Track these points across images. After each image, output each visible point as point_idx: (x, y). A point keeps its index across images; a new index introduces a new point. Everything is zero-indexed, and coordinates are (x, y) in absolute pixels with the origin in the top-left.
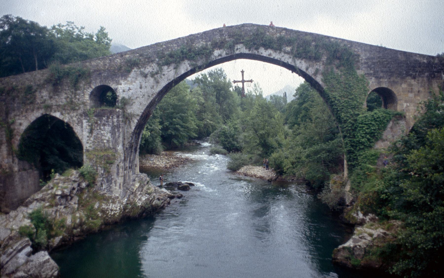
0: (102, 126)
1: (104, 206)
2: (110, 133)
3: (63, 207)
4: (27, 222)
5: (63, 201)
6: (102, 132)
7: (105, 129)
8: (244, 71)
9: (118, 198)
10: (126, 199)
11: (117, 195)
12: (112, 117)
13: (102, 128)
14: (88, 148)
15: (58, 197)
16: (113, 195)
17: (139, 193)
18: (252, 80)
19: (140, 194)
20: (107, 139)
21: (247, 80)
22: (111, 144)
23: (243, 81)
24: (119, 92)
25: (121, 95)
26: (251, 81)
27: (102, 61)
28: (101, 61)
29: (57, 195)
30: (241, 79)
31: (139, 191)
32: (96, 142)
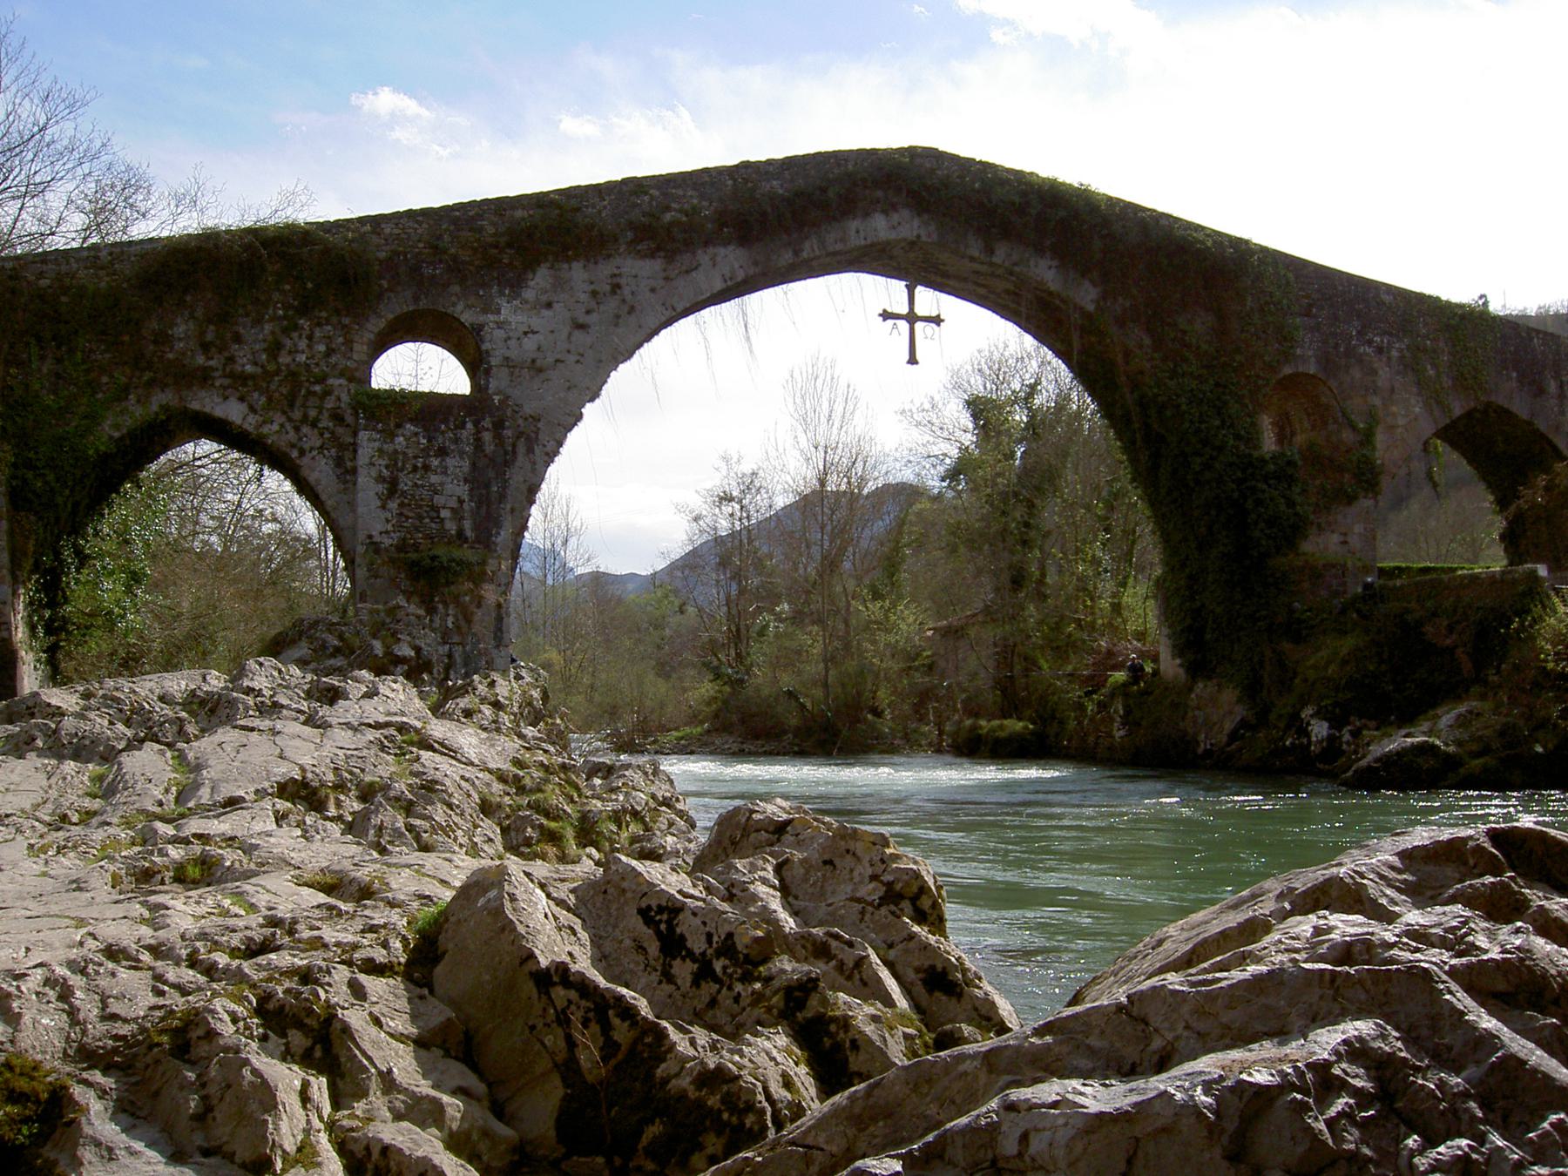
0: (436, 456)
2: (466, 481)
6: (434, 479)
7: (446, 468)
12: (476, 423)
13: (435, 462)
14: (377, 539)
18: (938, 316)
20: (453, 503)
21: (926, 314)
22: (467, 525)
23: (912, 318)
24: (488, 337)
27: (425, 226)
28: (417, 222)
32: (408, 518)
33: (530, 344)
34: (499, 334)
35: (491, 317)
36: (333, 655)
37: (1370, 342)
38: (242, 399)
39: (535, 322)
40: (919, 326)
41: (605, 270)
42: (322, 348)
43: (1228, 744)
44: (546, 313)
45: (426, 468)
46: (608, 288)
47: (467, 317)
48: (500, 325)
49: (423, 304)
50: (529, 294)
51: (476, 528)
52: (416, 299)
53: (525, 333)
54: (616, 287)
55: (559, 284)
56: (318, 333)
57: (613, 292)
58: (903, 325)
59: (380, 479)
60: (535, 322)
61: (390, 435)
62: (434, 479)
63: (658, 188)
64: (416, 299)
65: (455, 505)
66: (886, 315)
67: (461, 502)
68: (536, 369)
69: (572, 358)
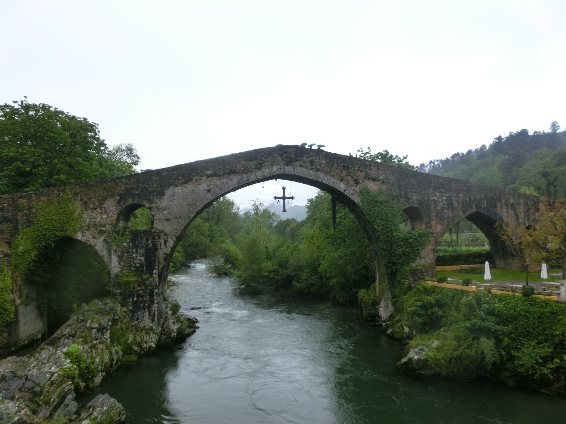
1: (138, 339)
2: (144, 256)
3: (98, 341)
4: (67, 363)
5: (99, 335)
8: (285, 188)
9: (151, 329)
10: (160, 329)
11: (151, 325)
15: (94, 331)
16: (146, 325)
19: (173, 322)
23: (284, 198)
26: (292, 198)
29: (94, 328)
30: (282, 195)
31: (172, 319)
36: (81, 322)
40: (286, 200)
43: (389, 321)
53: (164, 210)
58: (281, 201)
66: (276, 198)
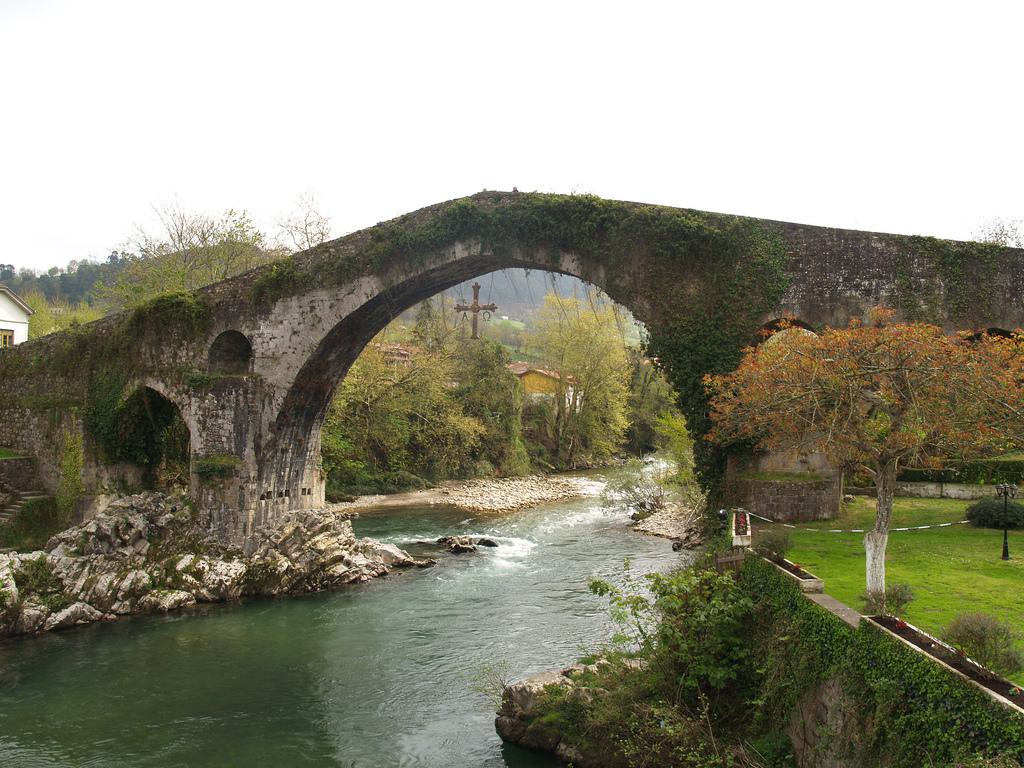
8: (479, 287)
12: (236, 392)
17: (295, 547)
20: (227, 435)
22: (233, 445)
25: (258, 347)
33: (272, 344)
34: (259, 340)
35: (257, 332)
37: (857, 287)
38: (163, 381)
39: (276, 332)
41: (306, 300)
42: (192, 354)
44: (280, 326)
45: (217, 416)
46: (309, 309)
47: (246, 333)
48: (260, 335)
49: (229, 327)
50: (272, 317)
51: (236, 448)
52: (227, 326)
54: (313, 308)
55: (286, 309)
56: (190, 346)
57: (311, 311)
58: (470, 315)
59: (199, 422)
60: (276, 332)
61: (202, 399)
62: (220, 421)
63: (334, 247)
64: (227, 326)
65: (227, 435)
67: (230, 433)
68: (274, 358)
69: (291, 350)
